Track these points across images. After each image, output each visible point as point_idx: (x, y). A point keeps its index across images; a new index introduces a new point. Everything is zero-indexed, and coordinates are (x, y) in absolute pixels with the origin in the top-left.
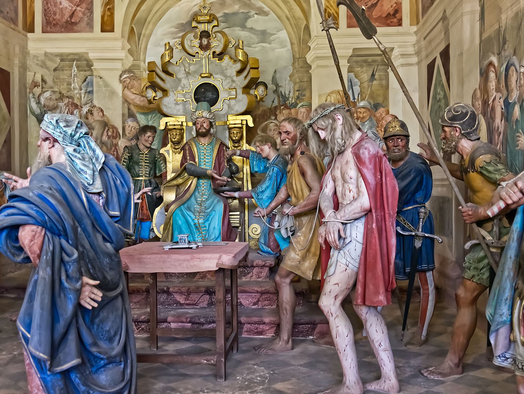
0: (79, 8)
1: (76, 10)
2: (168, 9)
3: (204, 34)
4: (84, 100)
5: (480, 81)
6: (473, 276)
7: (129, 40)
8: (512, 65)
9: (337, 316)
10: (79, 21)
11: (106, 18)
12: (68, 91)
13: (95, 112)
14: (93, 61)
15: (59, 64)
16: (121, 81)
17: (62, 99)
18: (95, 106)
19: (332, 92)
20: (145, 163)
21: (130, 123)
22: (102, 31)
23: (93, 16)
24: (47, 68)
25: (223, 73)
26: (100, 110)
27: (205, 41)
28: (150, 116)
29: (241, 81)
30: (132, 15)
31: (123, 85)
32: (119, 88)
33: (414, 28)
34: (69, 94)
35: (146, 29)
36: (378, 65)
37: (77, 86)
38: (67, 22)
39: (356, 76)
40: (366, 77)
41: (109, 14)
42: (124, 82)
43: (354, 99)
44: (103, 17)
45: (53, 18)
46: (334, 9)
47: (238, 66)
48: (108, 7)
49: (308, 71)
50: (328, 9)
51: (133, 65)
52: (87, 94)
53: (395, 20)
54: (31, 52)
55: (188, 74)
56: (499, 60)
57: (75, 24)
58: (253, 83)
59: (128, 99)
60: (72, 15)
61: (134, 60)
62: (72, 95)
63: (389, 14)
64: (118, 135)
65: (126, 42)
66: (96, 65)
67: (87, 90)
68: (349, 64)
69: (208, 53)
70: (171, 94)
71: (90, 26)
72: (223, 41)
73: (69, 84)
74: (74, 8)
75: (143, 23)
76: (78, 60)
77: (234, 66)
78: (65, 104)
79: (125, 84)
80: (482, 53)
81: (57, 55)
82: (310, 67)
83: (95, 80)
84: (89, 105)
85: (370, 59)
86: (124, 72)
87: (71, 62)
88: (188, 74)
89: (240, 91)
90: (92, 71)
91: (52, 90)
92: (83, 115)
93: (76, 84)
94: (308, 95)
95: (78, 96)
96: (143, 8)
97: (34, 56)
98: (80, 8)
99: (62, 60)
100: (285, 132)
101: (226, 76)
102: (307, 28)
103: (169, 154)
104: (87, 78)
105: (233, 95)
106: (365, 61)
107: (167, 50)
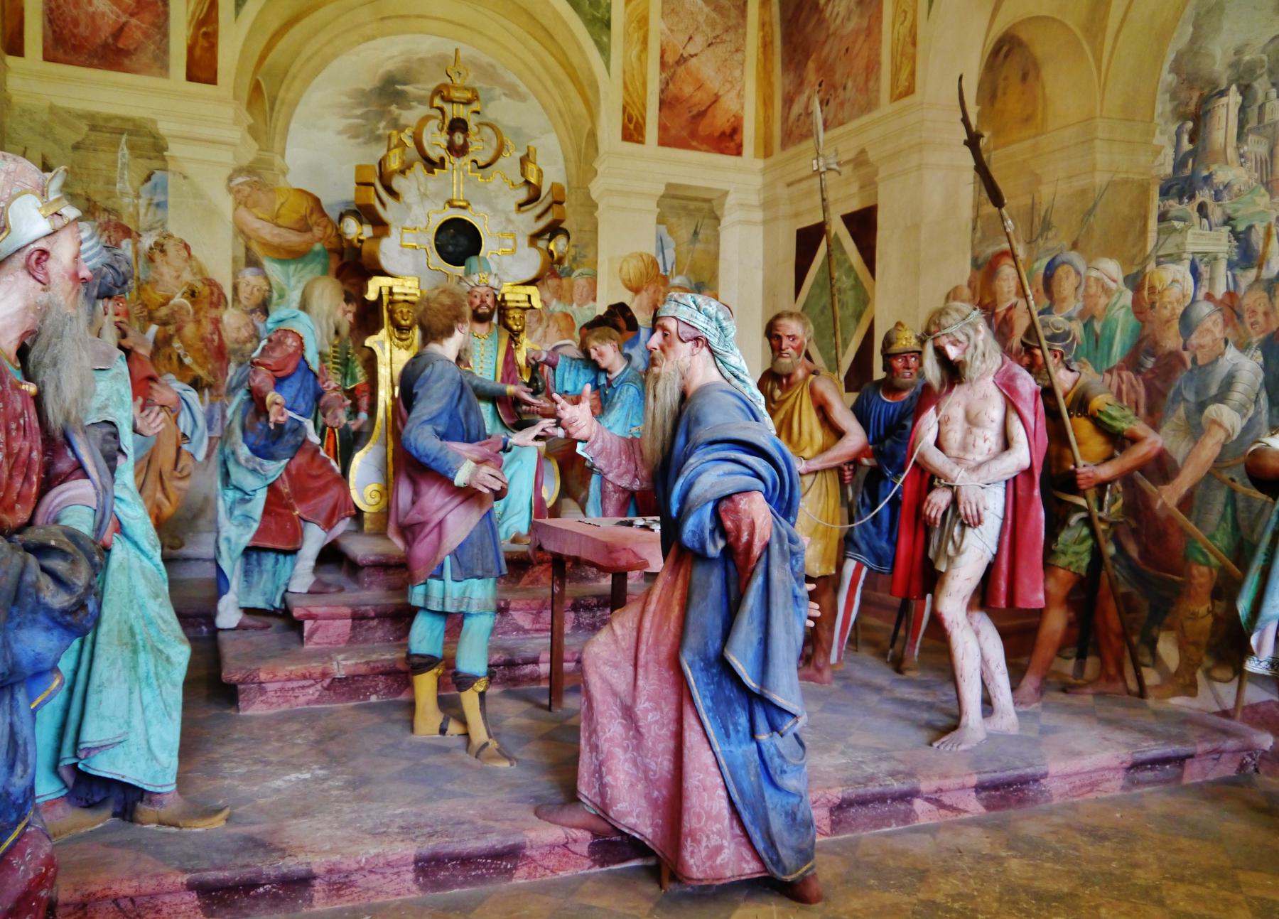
0: (134, 21)
1: (125, 24)
2: (335, 55)
3: (460, 125)
4: (144, 221)
5: (973, 276)
6: (1071, 563)
7: (250, 105)
8: (1064, 263)
9: (965, 627)
10: (136, 49)
11: (198, 52)
12: (108, 198)
13: (170, 247)
14: (168, 140)
15: (87, 136)
16: (230, 190)
17: (93, 214)
18: (170, 236)
19: (631, 256)
20: (334, 363)
21: (249, 276)
22: (191, 77)
23: (168, 42)
24: (56, 141)
25: (489, 202)
26: (182, 245)
27: (459, 139)
28: (292, 267)
29: (528, 222)
30: (256, 58)
31: (235, 199)
32: (226, 204)
33: (760, 164)
34: (110, 204)
35: (288, 89)
36: (704, 218)
37: (129, 189)
38: (105, 46)
39: (670, 232)
40: (685, 234)
41: (206, 44)
42: (238, 191)
43: (666, 270)
44: (191, 50)
45: (71, 31)
46: (638, 110)
47: (523, 194)
48: (204, 29)
49: (592, 214)
50: (628, 108)
51: (258, 160)
52: (152, 209)
53: (732, 145)
54: (15, 99)
55: (424, 196)
56: (1029, 253)
57: (126, 53)
58: (554, 230)
59: (246, 229)
60: (119, 32)
61: (261, 149)
62: (116, 207)
63: (723, 134)
64: (222, 300)
65: (244, 111)
66: (174, 150)
67: (151, 199)
68: (658, 210)
69: (466, 160)
70: (394, 231)
71: (161, 64)
72: (494, 143)
73: (110, 182)
74: (123, 19)
75: (281, 75)
76: (131, 133)
77: (513, 193)
78: (100, 225)
79: (240, 196)
80: (979, 234)
81: (81, 116)
82: (595, 206)
83: (171, 179)
84: (158, 231)
85: (692, 205)
86: (239, 171)
87: (114, 136)
88: (424, 196)
89: (524, 241)
90: (163, 159)
91: (70, 190)
92: (142, 253)
93: (127, 184)
94: (591, 255)
95: (131, 209)
96: (282, 44)
97: (24, 111)
98: (138, 19)
99: (93, 128)
100: (789, 337)
101: (494, 210)
102: (592, 135)
103: (383, 349)
104: (152, 173)
105: (509, 247)
106: (685, 208)
107: (396, 147)
